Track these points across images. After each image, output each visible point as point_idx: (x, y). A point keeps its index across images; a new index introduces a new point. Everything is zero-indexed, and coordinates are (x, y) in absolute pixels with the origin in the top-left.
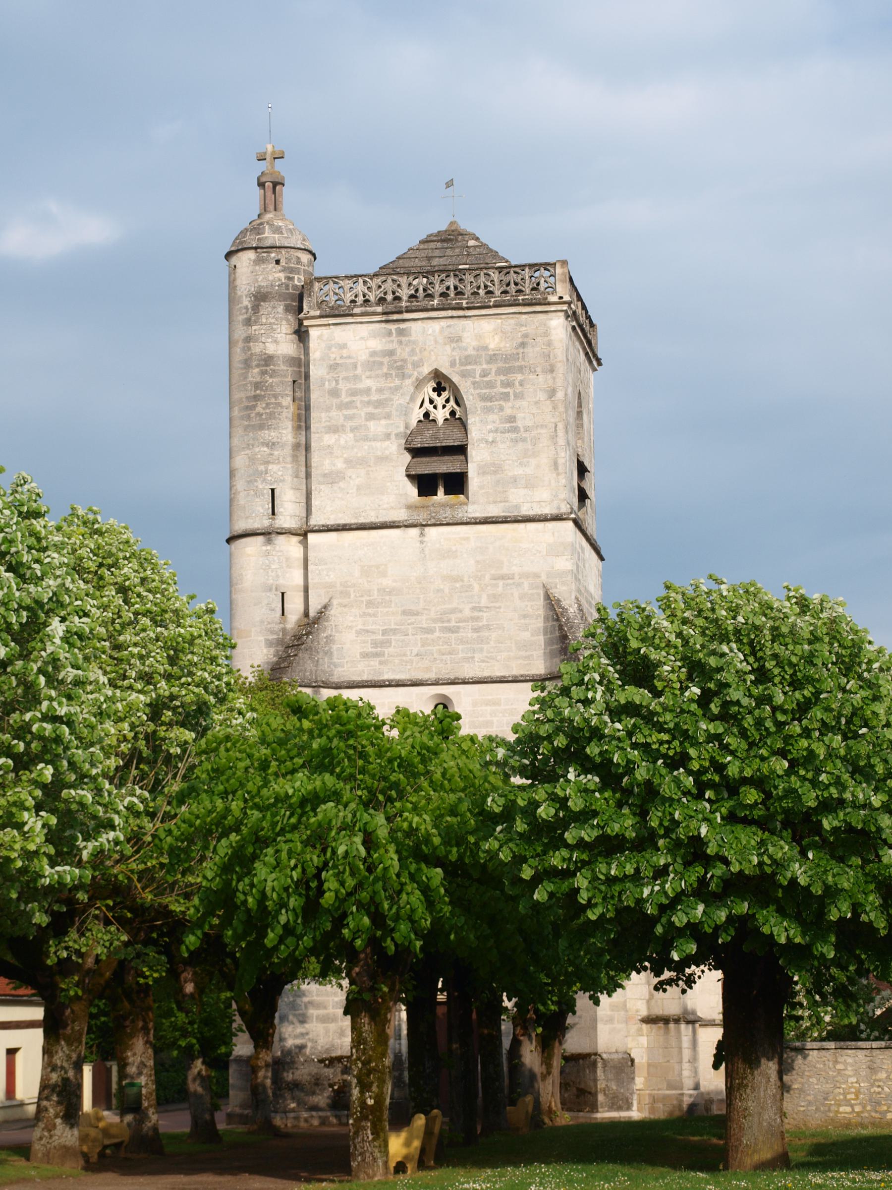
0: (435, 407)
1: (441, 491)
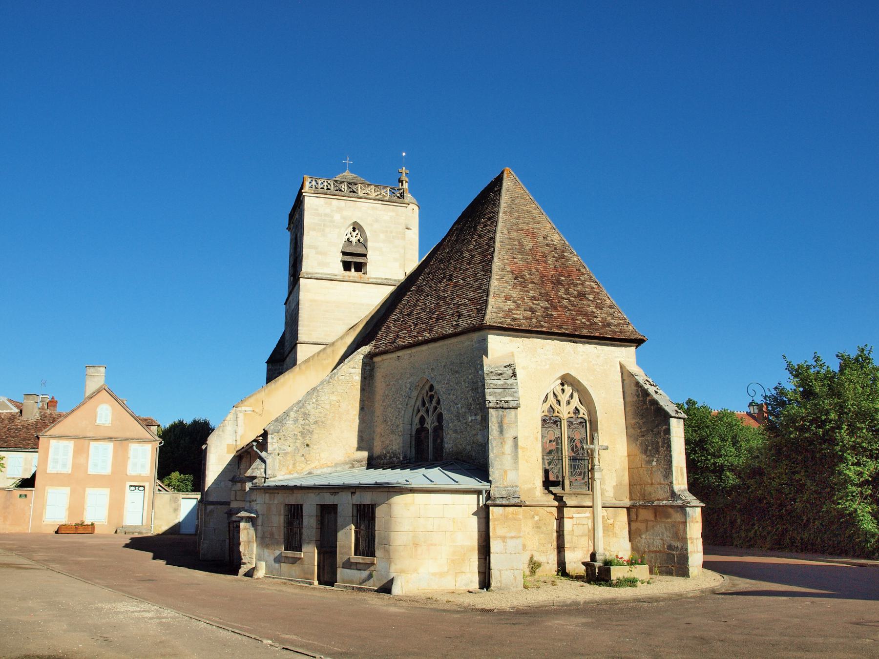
0: (352, 236)
1: (353, 270)
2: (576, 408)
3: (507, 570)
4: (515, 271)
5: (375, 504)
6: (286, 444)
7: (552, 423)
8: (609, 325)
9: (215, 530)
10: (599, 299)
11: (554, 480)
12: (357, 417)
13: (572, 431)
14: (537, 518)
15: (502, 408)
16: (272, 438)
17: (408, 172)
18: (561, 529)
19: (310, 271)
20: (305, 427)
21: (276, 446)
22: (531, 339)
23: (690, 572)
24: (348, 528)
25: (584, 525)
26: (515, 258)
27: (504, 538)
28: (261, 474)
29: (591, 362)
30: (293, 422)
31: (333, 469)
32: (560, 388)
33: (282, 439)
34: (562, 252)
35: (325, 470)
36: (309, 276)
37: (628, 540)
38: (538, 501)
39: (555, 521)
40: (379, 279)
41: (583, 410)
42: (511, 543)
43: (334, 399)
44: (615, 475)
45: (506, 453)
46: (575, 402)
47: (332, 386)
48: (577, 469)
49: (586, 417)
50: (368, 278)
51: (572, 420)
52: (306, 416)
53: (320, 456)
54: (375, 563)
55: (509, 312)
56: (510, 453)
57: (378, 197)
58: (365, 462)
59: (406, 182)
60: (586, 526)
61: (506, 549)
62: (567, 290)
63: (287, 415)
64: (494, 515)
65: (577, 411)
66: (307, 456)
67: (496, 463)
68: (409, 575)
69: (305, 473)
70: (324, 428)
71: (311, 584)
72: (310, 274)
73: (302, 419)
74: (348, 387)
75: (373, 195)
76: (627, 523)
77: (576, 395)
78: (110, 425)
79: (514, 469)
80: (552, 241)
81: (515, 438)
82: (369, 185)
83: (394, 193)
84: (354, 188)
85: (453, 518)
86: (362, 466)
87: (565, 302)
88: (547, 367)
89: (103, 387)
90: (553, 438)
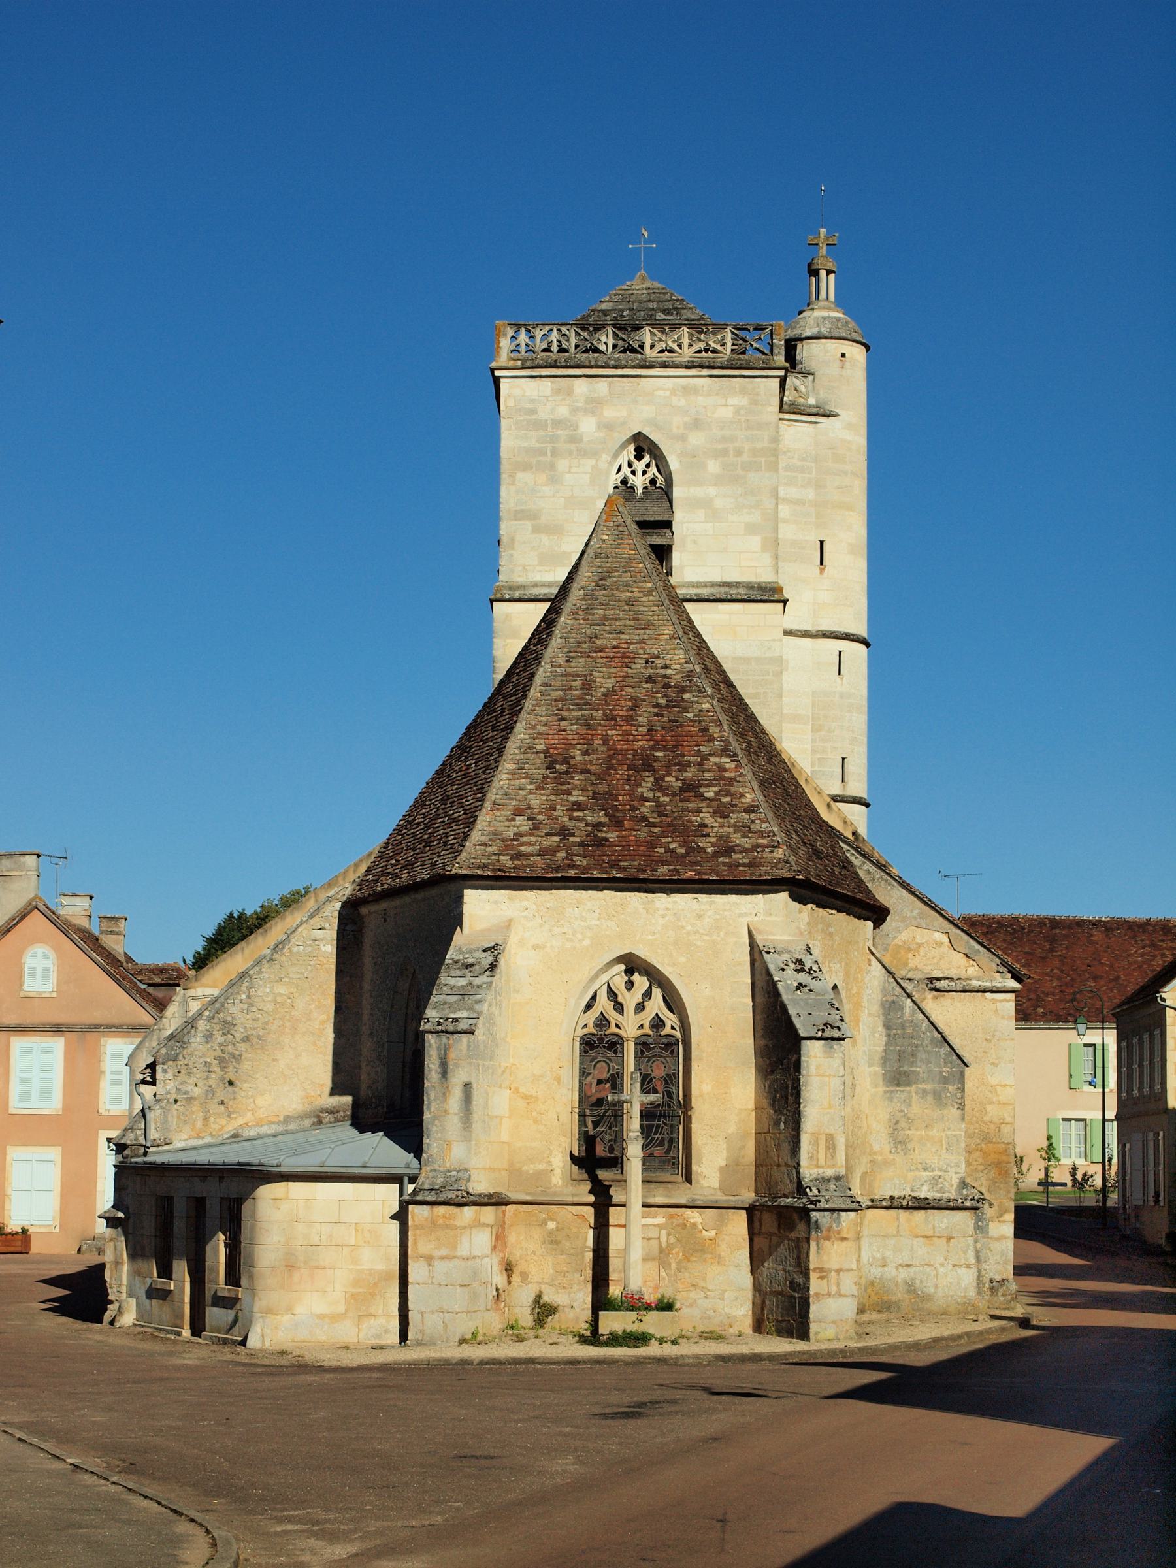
0: (633, 473)
2: (657, 1014)
3: (433, 1312)
4: (555, 748)
5: (241, 1198)
7: (604, 1047)
8: (730, 850)
10: (728, 794)
13: (648, 1062)
14: (551, 1225)
15: (447, 1032)
16: (165, 1071)
19: (519, 579)
20: (226, 1048)
21: (171, 1085)
22: (553, 891)
23: (811, 1330)
24: (215, 1238)
27: (429, 1259)
28: (136, 1139)
29: (683, 927)
30: (203, 1040)
31: (281, 1128)
32: (619, 982)
33: (182, 1071)
34: (678, 692)
35: (265, 1130)
36: (517, 595)
38: (555, 1193)
39: (592, 1230)
40: (705, 585)
41: (670, 1019)
42: (440, 1267)
44: (725, 1146)
45: (451, 1111)
46: (656, 1004)
47: (278, 966)
48: (655, 1134)
49: (678, 1034)
51: (650, 1040)
52: (228, 1027)
53: (254, 1102)
54: (240, 1297)
56: (457, 1111)
59: (829, 272)
60: (655, 1243)
61: (433, 1277)
62: (658, 781)
63: (193, 1027)
64: (416, 1219)
65: (658, 1023)
67: (434, 1129)
68: (279, 1317)
69: (226, 1136)
70: (262, 1048)
71: (179, 1334)
72: (519, 587)
73: (221, 1032)
75: (687, 354)
77: (657, 993)
78: (54, 995)
79: (463, 1139)
80: (666, 667)
81: (467, 1086)
82: (675, 327)
83: (746, 341)
87: (646, 809)
88: (587, 942)
89: (34, 903)
90: (605, 1076)
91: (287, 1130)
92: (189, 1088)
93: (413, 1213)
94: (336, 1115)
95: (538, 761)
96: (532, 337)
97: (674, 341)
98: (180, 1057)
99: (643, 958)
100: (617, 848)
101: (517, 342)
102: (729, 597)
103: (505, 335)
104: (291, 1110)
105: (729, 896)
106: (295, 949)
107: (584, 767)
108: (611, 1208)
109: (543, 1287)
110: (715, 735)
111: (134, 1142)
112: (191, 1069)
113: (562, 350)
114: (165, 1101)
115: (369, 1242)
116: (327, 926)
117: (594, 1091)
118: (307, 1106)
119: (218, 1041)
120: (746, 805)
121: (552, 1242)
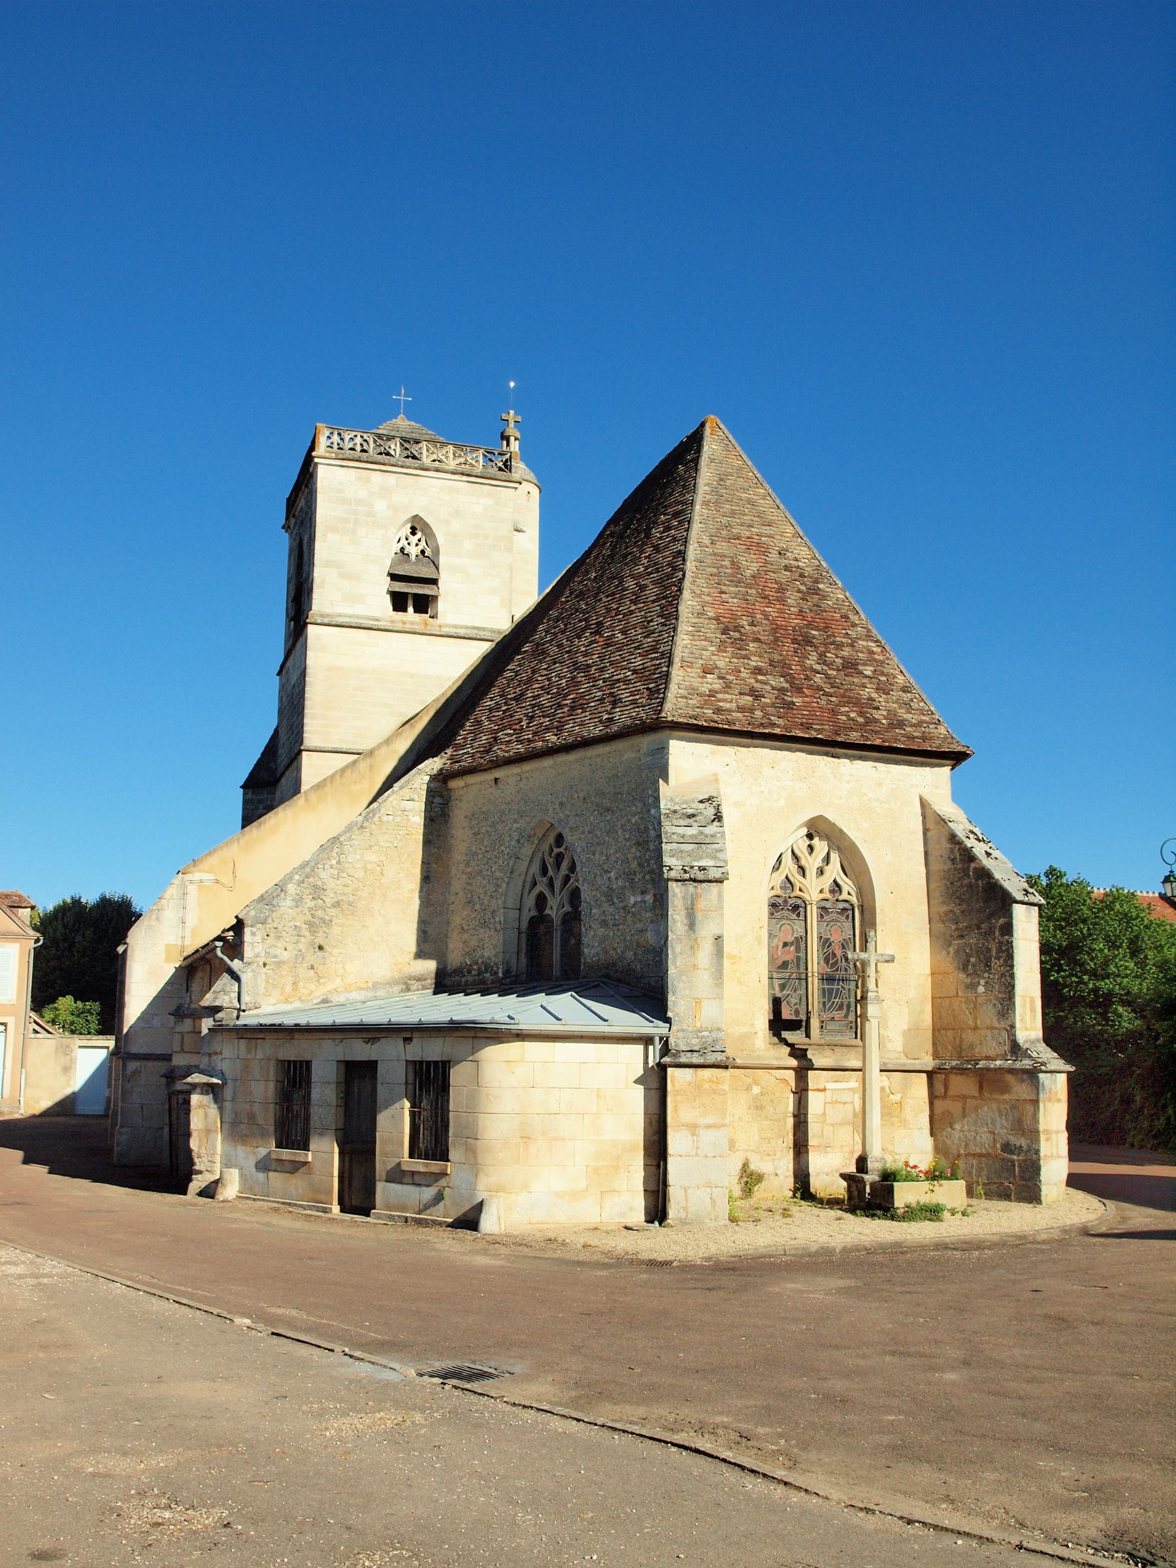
0: (409, 544)
1: (411, 609)
2: (835, 881)
4: (724, 617)
5: (449, 1061)
6: (280, 945)
8: (901, 724)
9: (142, 1107)
10: (882, 674)
11: (790, 1017)
12: (416, 895)
15: (695, 880)
16: (253, 934)
17: (519, 419)
18: (802, 1111)
20: (316, 913)
21: (259, 949)
22: (751, 749)
23: (1042, 1193)
24: (397, 1105)
25: (845, 1103)
26: (725, 593)
27: (693, 1128)
28: (231, 1002)
30: (293, 904)
32: (802, 846)
33: (272, 935)
34: (814, 582)
35: (355, 996)
36: (326, 621)
37: (929, 1132)
39: (792, 1095)
40: (462, 627)
41: (847, 885)
42: (706, 1136)
43: (373, 860)
45: (701, 966)
46: (834, 870)
47: (368, 834)
48: (835, 998)
49: (854, 900)
50: (440, 626)
51: (828, 905)
52: (318, 892)
53: (344, 968)
54: (449, 1172)
55: (709, 696)
56: (707, 967)
57: (460, 469)
58: (431, 981)
60: (849, 1107)
62: (822, 655)
64: (676, 1084)
65: (837, 887)
66: (320, 968)
68: (514, 1195)
69: (315, 1001)
72: (328, 616)
73: (311, 897)
74: (399, 837)
75: (452, 464)
76: (927, 1100)
77: (835, 858)
79: (715, 996)
80: (796, 560)
81: (718, 938)
82: (444, 445)
84: (414, 449)
85: (598, 1089)
86: (424, 988)
87: (818, 679)
90: (790, 939)
91: (375, 997)
92: (278, 952)
93: (673, 1077)
94: (423, 983)
95: (713, 626)
96: (342, 439)
97: (443, 455)
98: (270, 921)
99: (832, 821)
100: (805, 712)
101: (331, 441)
102: (479, 637)
103: (324, 434)
104: (379, 976)
105: (902, 766)
106: (385, 818)
107: (755, 636)
108: (810, 1073)
109: (749, 1155)
110: (856, 622)
111: (230, 1005)
112: (280, 933)
113: (363, 451)
114: (256, 964)
115: (612, 1110)
116: (416, 797)
117: (780, 954)
118: (395, 973)
119: (308, 905)
120: (901, 685)
121: (757, 1108)
